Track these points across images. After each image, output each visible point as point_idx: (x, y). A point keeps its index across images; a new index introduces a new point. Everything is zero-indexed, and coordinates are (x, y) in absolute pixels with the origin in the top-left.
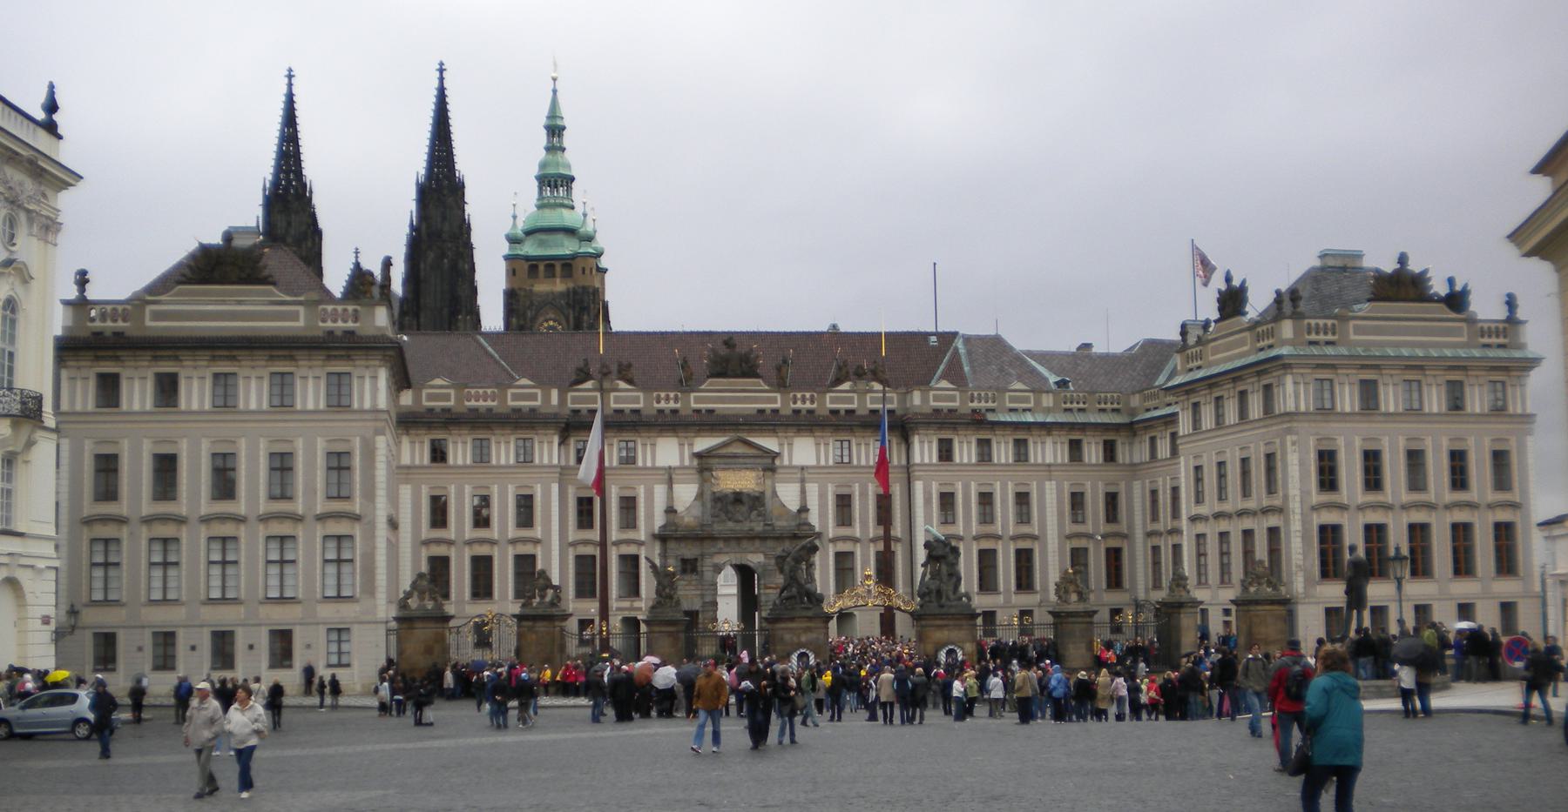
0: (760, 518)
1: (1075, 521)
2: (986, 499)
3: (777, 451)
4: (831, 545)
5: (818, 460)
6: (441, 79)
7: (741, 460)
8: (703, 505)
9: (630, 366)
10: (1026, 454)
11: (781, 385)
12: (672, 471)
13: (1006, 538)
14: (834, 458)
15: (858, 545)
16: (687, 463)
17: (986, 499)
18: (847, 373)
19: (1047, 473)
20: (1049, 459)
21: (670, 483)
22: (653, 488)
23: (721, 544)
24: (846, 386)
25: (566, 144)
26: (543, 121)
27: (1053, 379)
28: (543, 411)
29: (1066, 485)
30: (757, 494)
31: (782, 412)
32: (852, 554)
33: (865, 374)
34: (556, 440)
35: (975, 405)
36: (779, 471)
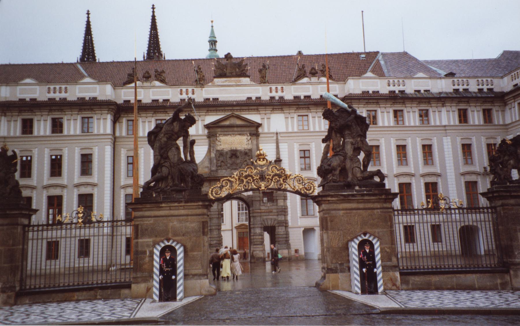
1: (466, 163)
2: (402, 149)
3: (260, 123)
5: (287, 128)
6: (153, 12)
7: (235, 129)
9: (163, 72)
10: (428, 120)
11: (263, 80)
13: (418, 175)
14: (298, 128)
17: (402, 149)
18: (305, 72)
19: (444, 132)
20: (445, 122)
24: (305, 80)
25: (217, 48)
26: (208, 39)
27: (443, 73)
28: (99, 98)
29: (459, 139)
30: (247, 151)
31: (262, 99)
34: (109, 118)
35: (392, 88)
36: (261, 135)
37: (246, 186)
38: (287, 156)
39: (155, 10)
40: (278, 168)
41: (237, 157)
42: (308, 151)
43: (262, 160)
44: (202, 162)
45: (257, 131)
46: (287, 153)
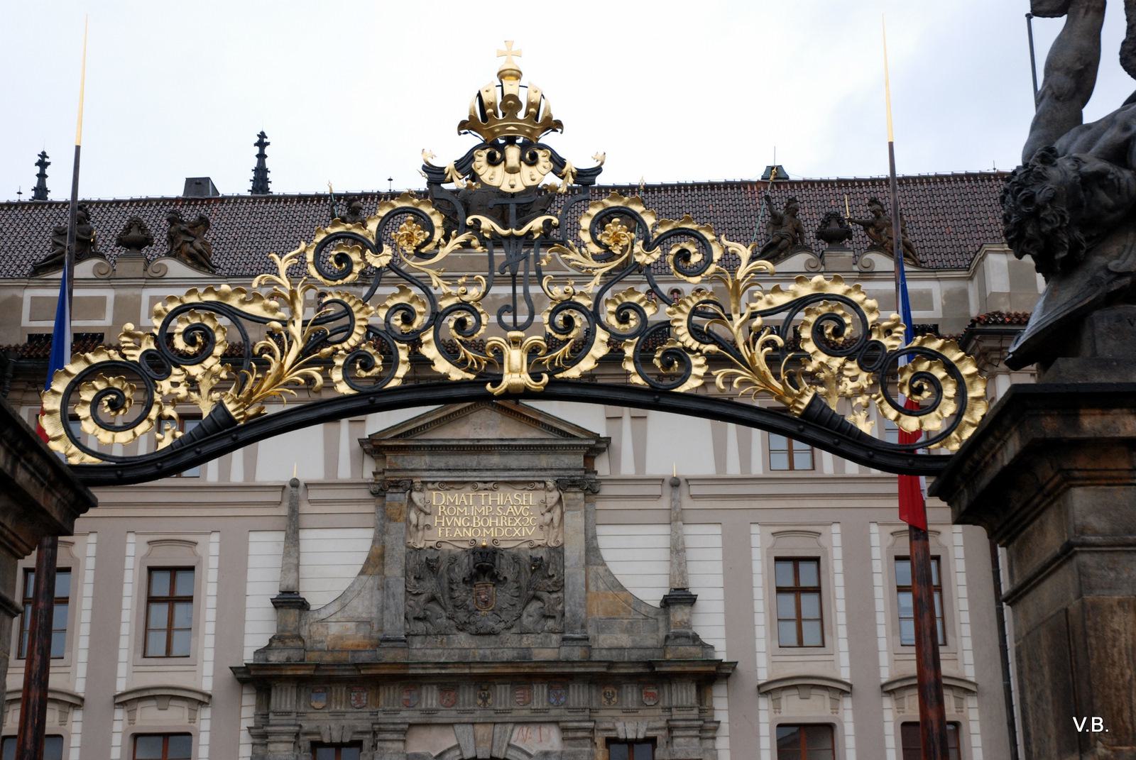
0: (550, 623)
4: (764, 703)
6: (262, 156)
7: (495, 460)
8: (384, 587)
12: (301, 491)
15: (847, 703)
16: (345, 472)
18: (798, 230)
21: (293, 529)
22: (246, 542)
23: (431, 698)
30: (541, 553)
32: (827, 730)
33: (848, 234)
36: (606, 490)
37: (367, 366)
38: (719, 581)
39: (267, 150)
40: (649, 220)
41: (497, 580)
42: (813, 566)
43: (513, 154)
44: (343, 600)
45: (589, 467)
46: (719, 567)
